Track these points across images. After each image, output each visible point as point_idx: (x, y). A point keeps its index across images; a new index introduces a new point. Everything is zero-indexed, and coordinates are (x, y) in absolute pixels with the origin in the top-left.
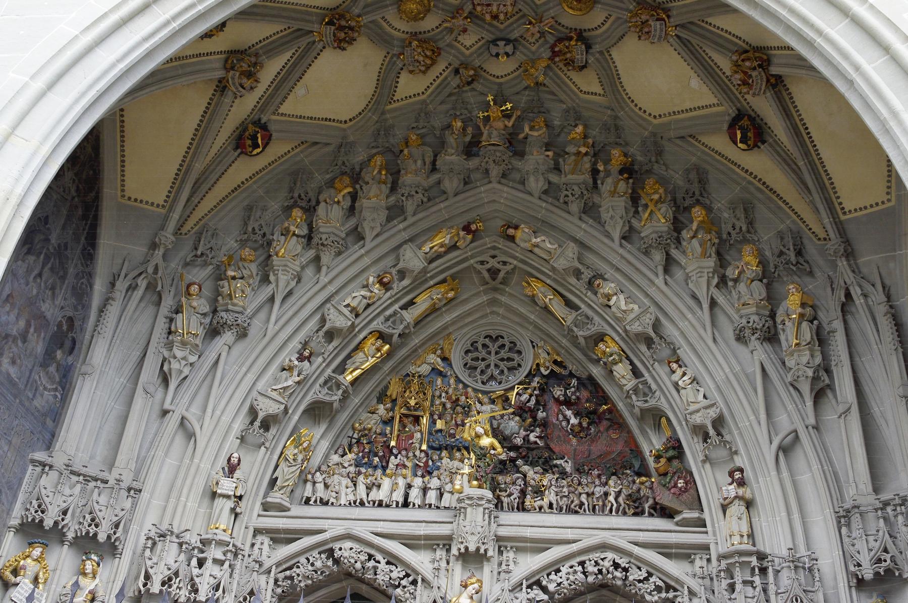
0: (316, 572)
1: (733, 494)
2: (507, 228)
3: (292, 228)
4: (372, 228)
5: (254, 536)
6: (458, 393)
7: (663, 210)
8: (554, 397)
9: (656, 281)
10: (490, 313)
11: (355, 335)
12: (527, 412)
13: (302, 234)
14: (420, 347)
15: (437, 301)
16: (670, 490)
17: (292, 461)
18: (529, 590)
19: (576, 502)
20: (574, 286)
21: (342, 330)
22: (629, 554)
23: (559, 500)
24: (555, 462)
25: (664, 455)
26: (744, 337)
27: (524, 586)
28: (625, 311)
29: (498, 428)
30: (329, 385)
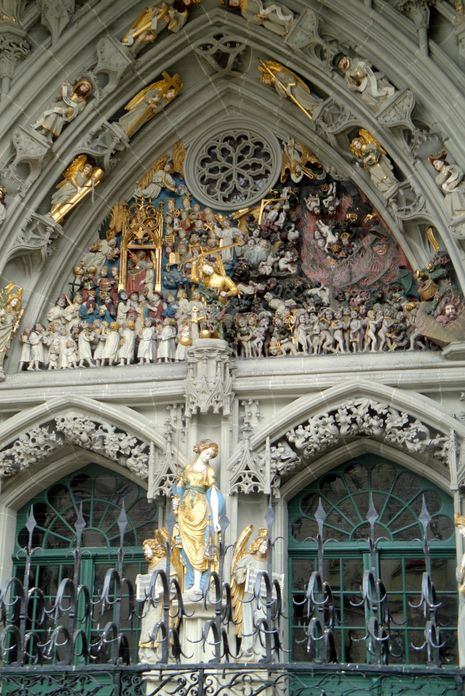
0: (38, 447)
4: (59, 19)
6: (193, 217)
9: (417, 52)
10: (227, 108)
11: (58, 161)
14: (143, 163)
15: (154, 106)
18: (274, 448)
19: (330, 340)
21: (36, 160)
24: (310, 292)
25: (429, 275)
27: (268, 444)
28: (377, 98)
29: (242, 256)
30: (34, 227)
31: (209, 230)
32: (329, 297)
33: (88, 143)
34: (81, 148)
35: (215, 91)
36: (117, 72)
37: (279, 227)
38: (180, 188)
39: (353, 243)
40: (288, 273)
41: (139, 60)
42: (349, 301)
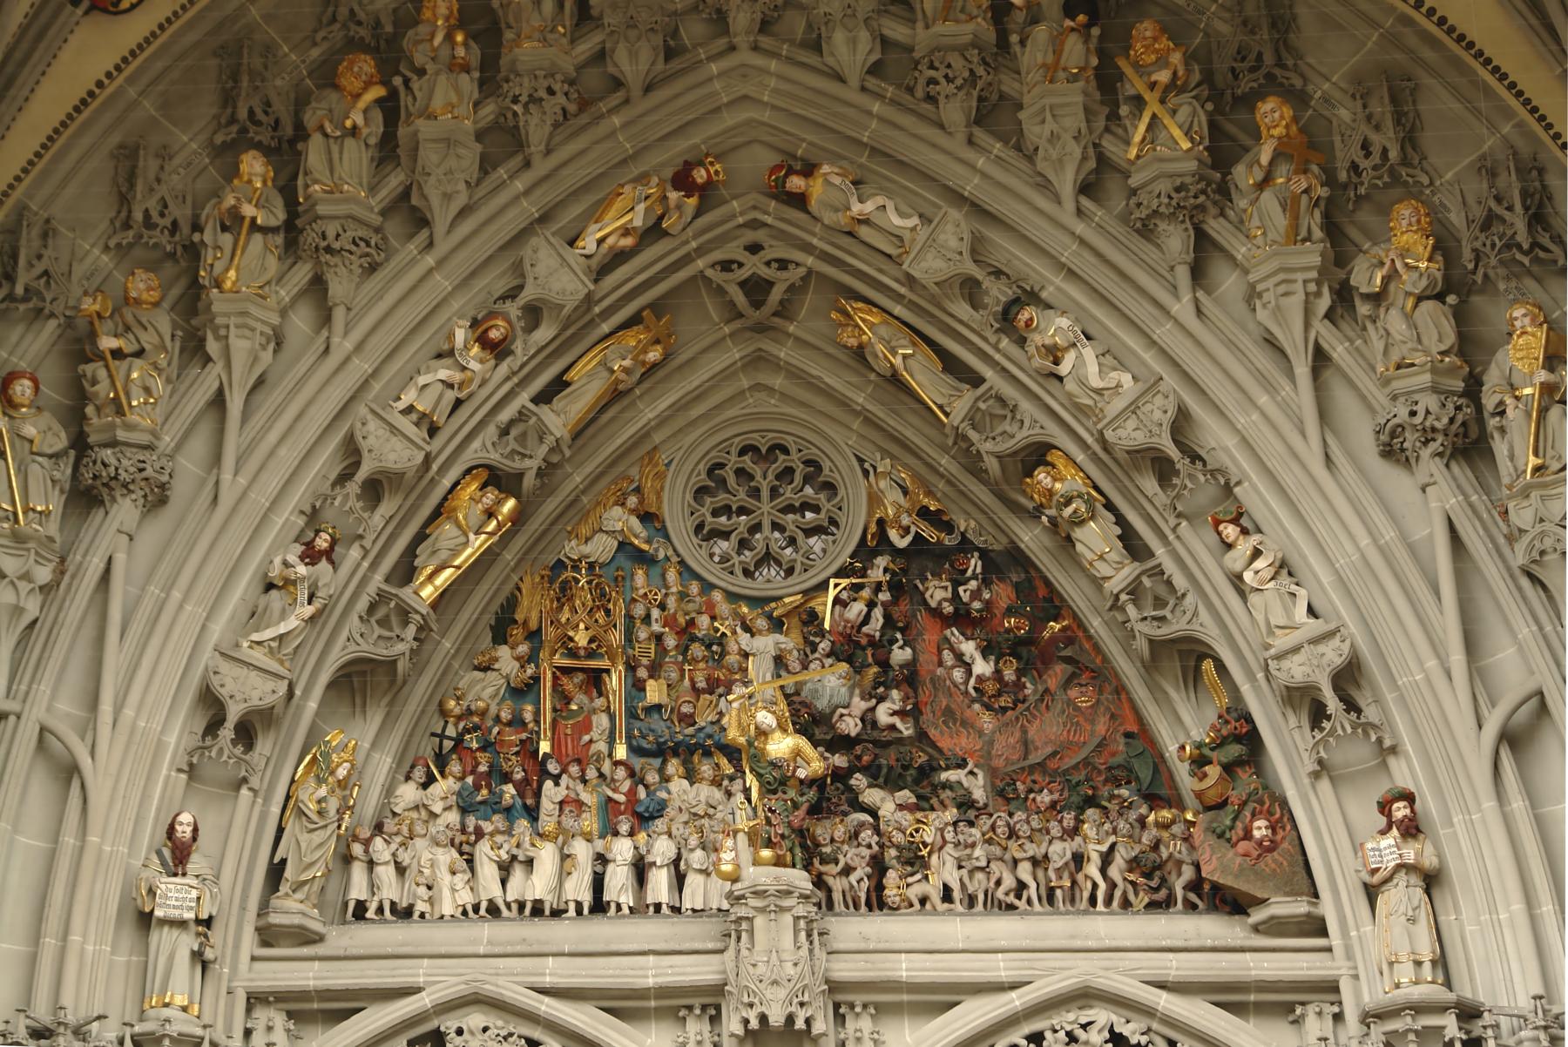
5: (249, 1010)
6: (691, 606)
8: (925, 600)
10: (751, 388)
13: (273, 222)
17: (314, 817)
20: (961, 322)
33: (493, 444)
41: (601, 283)
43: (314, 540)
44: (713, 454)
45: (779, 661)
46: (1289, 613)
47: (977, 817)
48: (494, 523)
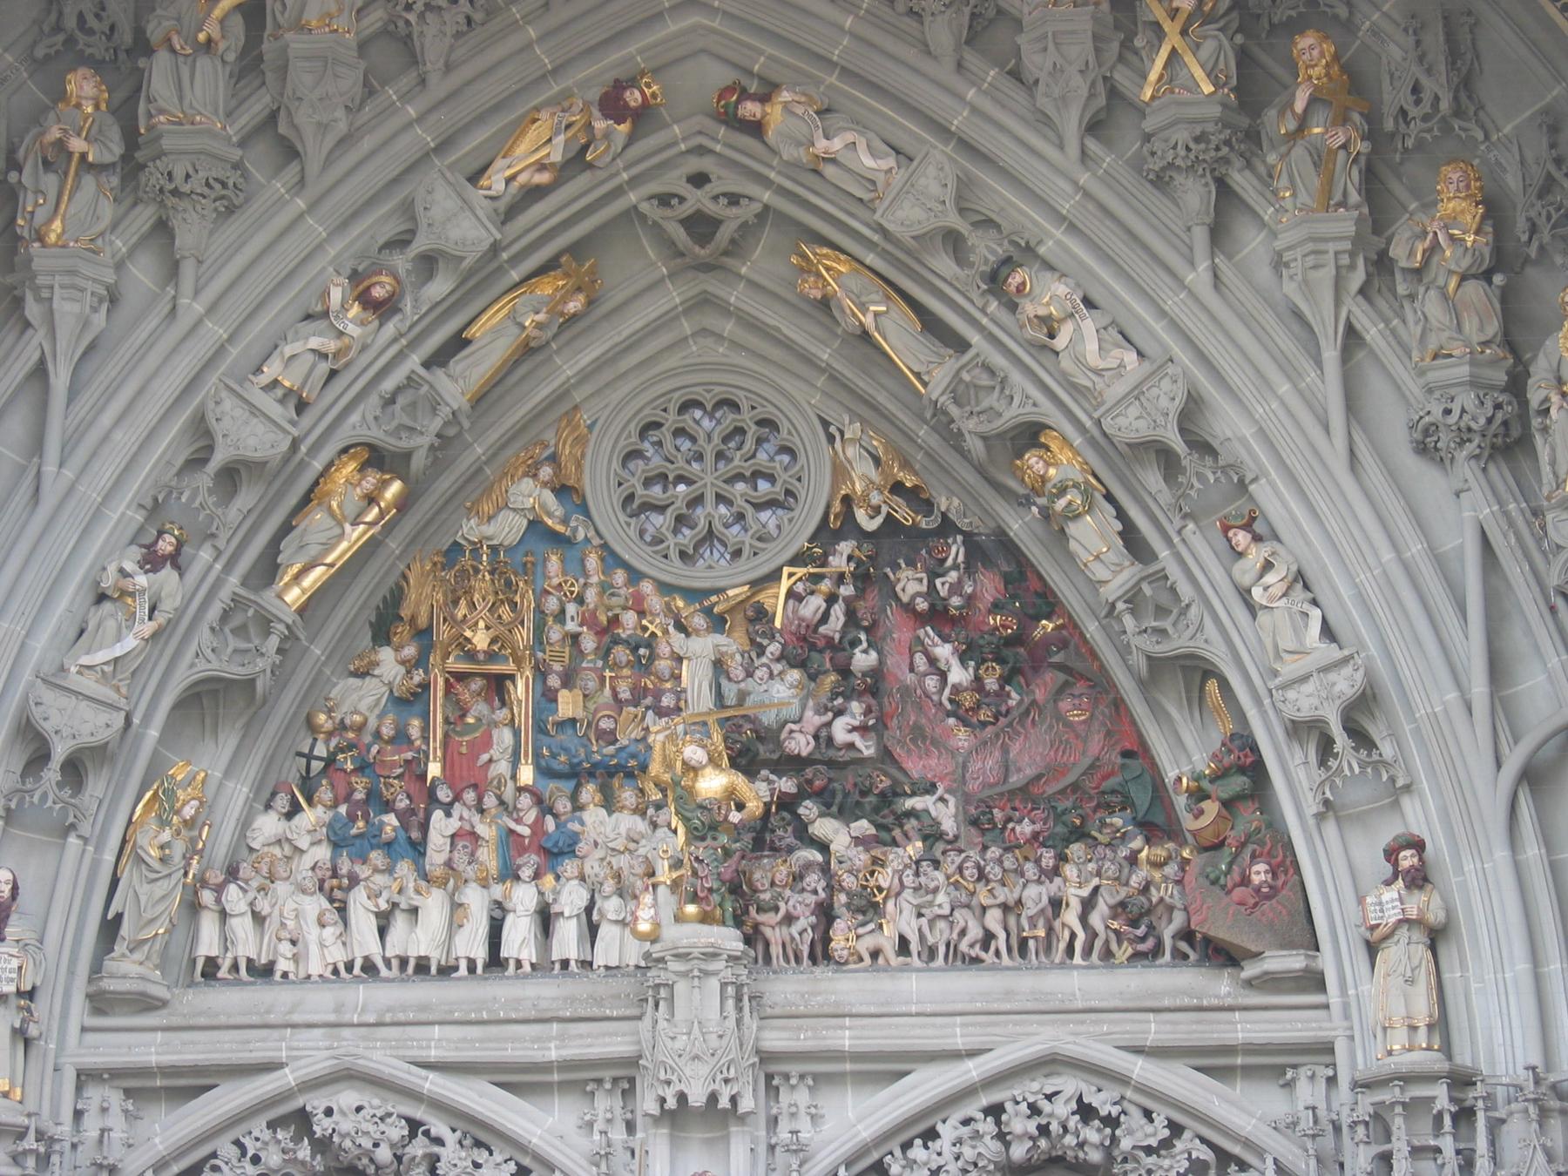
1: (1392, 916)
2: (738, 102)
3: (77, 145)
4: (323, 128)
5: (79, 1089)
7: (1208, 47)
9: (1190, 278)
12: (821, 651)
15: (536, 333)
16: (1229, 892)
17: (156, 865)
19: (975, 932)
22: (1122, 1080)
23: (926, 929)
24: (910, 803)
26: (1436, 449)
28: (1098, 372)
30: (237, 620)
31: (653, 634)
32: (956, 816)
33: (376, 418)
34: (359, 431)
35: (674, 296)
36: (462, 259)
37: (829, 640)
38: (573, 524)
39: (1008, 688)
40: (853, 754)
42: (1004, 828)
43: (156, 542)
44: (646, 411)
45: (719, 665)
46: (1298, 633)
47: (944, 853)
48: (376, 510)
